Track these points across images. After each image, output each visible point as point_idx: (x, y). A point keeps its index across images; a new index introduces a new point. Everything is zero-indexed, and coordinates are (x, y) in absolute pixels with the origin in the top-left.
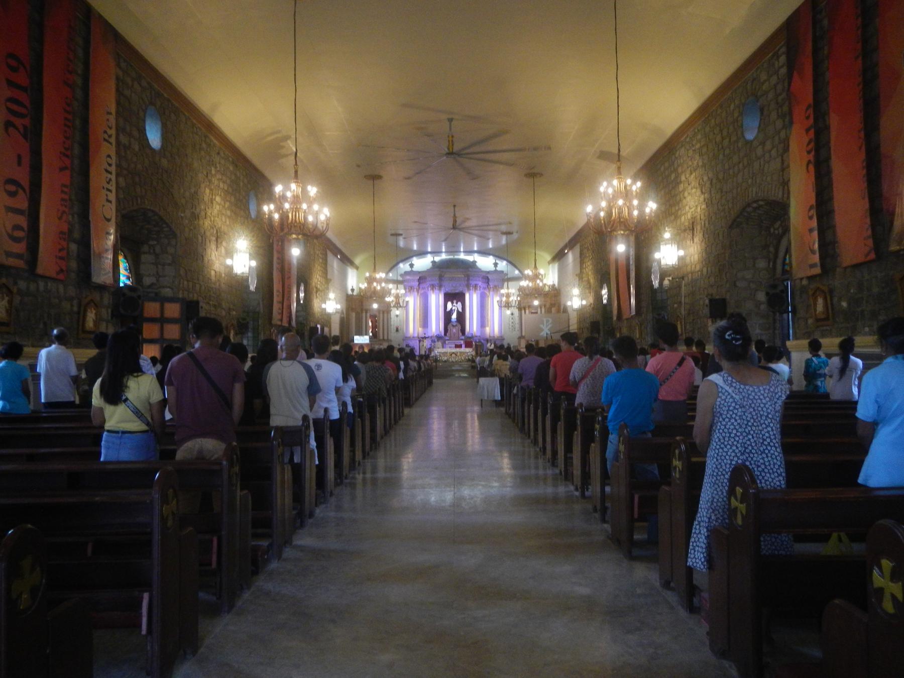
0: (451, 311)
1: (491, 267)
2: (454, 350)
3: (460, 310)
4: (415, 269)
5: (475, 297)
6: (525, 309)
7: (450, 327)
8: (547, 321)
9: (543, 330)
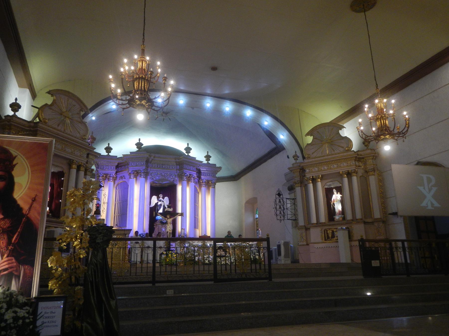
4: (112, 154)
6: (314, 181)
8: (429, 180)
9: (425, 197)
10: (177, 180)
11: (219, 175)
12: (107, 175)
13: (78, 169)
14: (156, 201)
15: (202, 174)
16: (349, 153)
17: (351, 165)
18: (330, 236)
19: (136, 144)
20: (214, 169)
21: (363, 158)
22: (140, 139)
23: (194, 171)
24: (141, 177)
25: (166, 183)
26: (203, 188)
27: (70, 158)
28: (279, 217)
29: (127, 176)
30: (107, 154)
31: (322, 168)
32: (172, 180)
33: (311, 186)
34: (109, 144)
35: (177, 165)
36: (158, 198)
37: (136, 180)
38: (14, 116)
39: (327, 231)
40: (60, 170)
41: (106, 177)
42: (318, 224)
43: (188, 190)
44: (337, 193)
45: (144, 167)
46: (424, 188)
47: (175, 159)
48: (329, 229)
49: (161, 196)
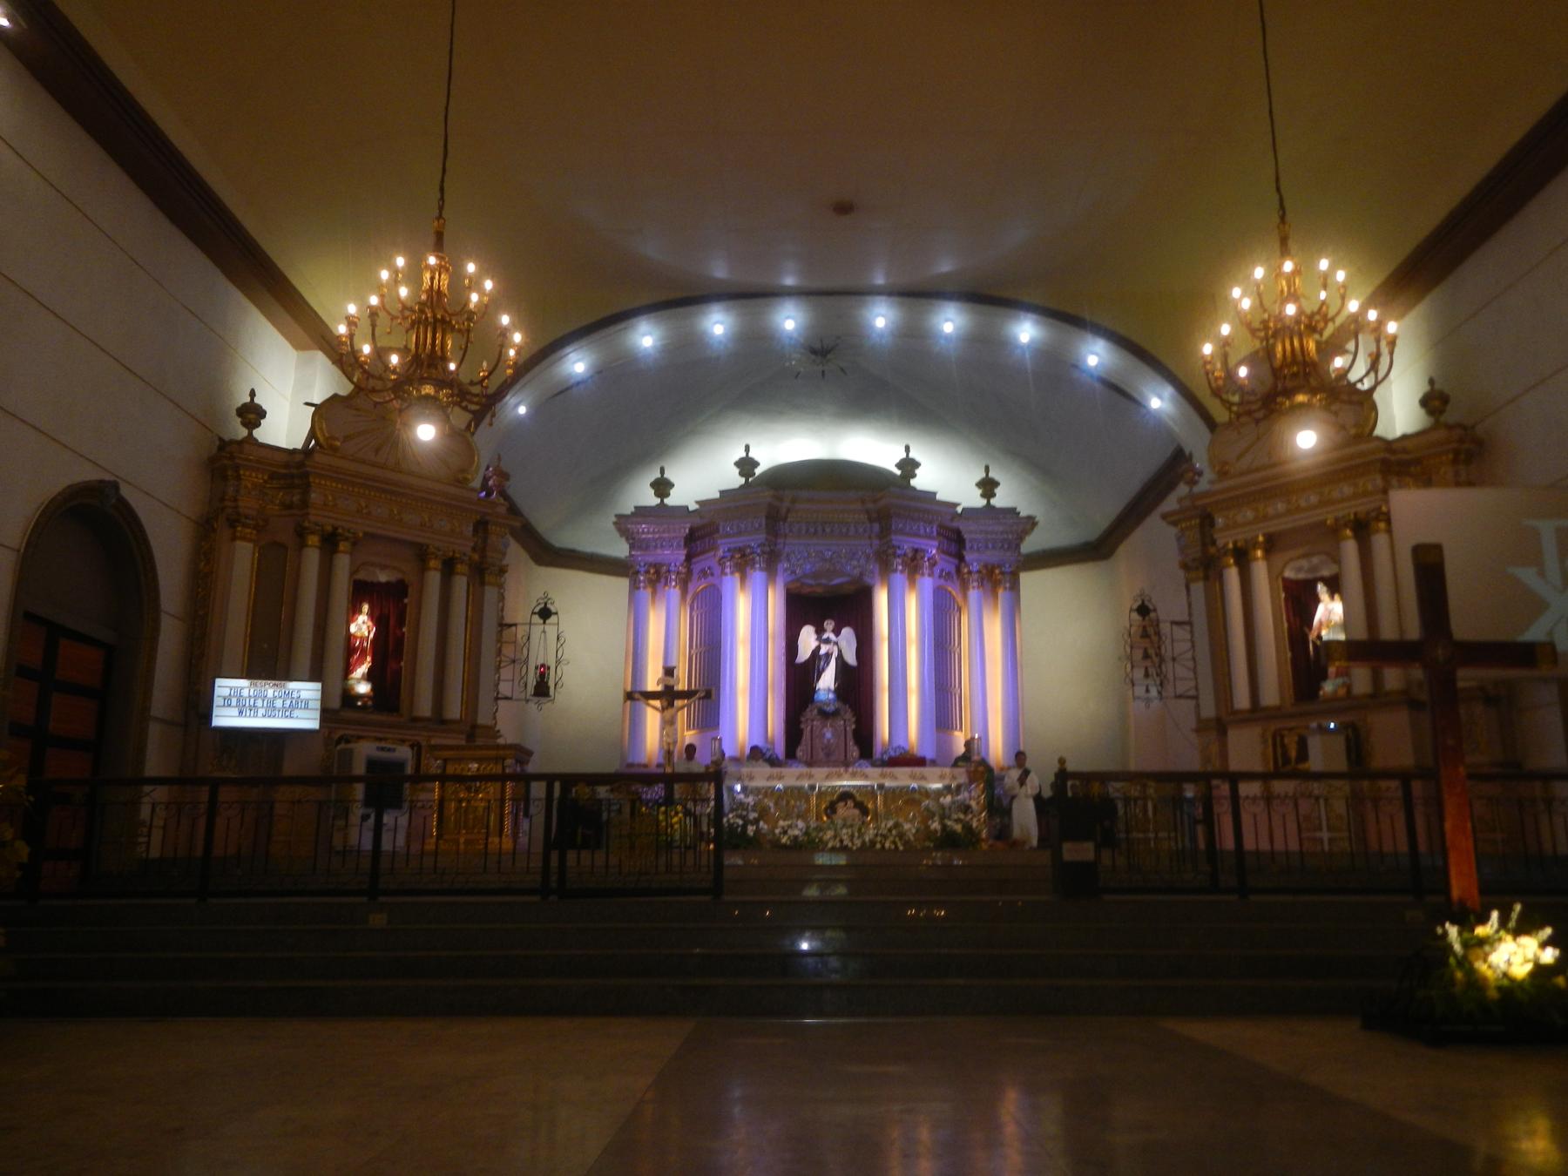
0: (815, 664)
1: (971, 498)
2: (846, 783)
3: (851, 659)
5: (912, 604)
6: (1242, 557)
7: (810, 718)
10: (872, 572)
11: (1030, 544)
12: (657, 567)
13: (449, 567)
14: (813, 644)
15: (968, 545)
16: (1364, 447)
17: (1365, 494)
18: (1293, 754)
19: (738, 464)
20: (1016, 524)
21: (1418, 462)
22: (747, 448)
23: (929, 537)
24: (753, 566)
25: (841, 584)
26: (973, 594)
27: (419, 540)
28: (1140, 691)
29: (717, 570)
30: (658, 501)
31: (1271, 511)
32: (856, 572)
33: (1232, 575)
34: (662, 471)
35: (871, 520)
36: (820, 631)
37: (743, 580)
38: (250, 439)
39: (1282, 737)
40: (400, 576)
41: (657, 572)
42: (1257, 712)
43: (912, 604)
44: (1332, 598)
45: (762, 537)
46: (1542, 574)
47: (863, 502)
48: (1291, 729)
49: (829, 625)
